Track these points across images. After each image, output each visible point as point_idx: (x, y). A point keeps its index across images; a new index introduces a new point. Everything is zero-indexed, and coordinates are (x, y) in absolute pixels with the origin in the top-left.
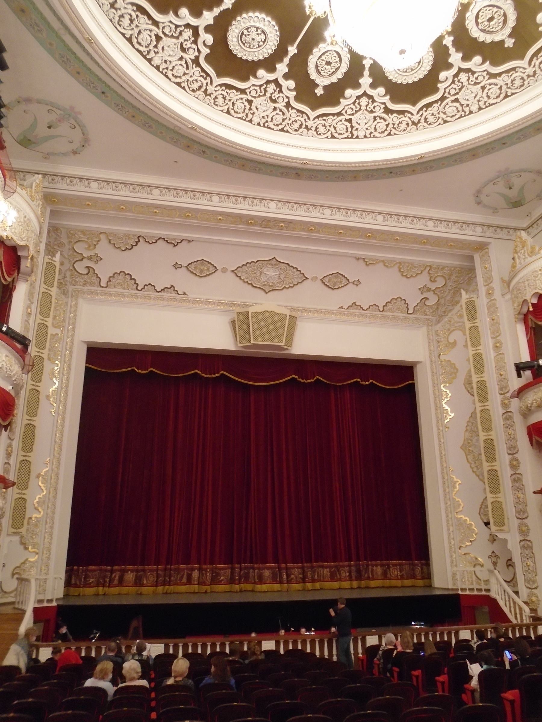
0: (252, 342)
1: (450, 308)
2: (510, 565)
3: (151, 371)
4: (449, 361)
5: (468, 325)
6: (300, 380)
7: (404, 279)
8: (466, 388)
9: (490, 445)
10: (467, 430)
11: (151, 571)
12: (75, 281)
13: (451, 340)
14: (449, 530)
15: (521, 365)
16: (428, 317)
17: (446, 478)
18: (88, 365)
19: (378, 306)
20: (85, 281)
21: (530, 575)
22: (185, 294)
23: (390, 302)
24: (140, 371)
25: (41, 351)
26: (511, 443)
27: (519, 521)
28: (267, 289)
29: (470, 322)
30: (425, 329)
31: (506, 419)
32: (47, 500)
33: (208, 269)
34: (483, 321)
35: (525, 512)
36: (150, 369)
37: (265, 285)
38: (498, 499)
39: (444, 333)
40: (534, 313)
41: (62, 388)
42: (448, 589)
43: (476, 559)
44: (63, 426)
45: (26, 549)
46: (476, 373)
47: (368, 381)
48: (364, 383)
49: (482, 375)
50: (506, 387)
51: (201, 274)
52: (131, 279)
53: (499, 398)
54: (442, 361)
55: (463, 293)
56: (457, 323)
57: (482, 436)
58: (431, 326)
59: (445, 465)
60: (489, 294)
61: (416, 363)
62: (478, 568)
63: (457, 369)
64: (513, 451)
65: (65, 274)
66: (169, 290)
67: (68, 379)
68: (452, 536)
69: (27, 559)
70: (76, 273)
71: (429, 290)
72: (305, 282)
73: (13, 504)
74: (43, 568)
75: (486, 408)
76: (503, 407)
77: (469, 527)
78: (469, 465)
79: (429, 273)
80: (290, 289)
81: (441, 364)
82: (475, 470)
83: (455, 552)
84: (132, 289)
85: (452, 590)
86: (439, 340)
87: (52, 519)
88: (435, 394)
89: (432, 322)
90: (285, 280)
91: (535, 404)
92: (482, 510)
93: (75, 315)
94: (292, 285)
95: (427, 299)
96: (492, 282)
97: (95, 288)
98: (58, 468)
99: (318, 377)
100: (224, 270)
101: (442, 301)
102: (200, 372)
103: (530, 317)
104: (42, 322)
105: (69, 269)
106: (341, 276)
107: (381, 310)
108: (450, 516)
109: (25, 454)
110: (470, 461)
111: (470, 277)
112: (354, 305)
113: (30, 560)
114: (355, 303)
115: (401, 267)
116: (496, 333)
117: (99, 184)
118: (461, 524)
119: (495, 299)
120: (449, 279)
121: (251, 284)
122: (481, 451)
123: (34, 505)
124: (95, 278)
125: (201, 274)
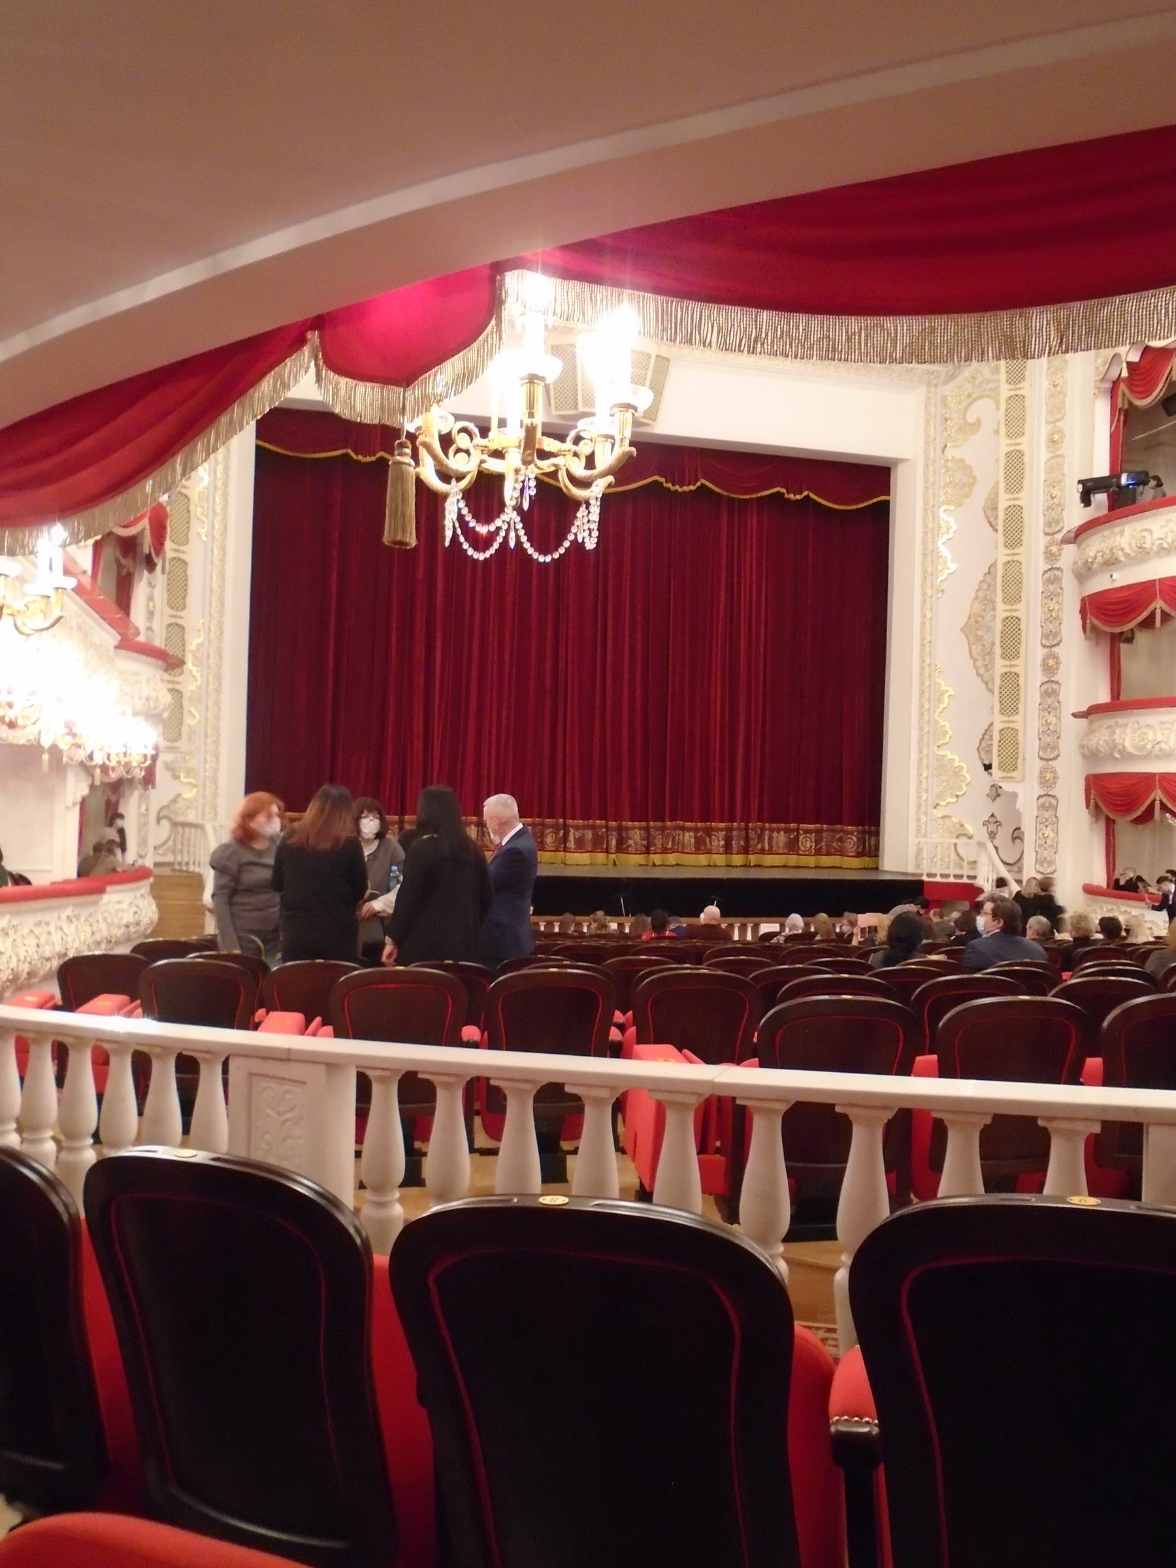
2: (1018, 837)
4: (961, 460)
5: (1005, 391)
6: (669, 485)
8: (987, 517)
9: (1012, 627)
10: (976, 598)
13: (971, 418)
15: (1090, 484)
18: (260, 443)
21: (1046, 853)
24: (360, 458)
26: (1051, 626)
27: (1043, 763)
30: (922, 390)
31: (1049, 582)
35: (1055, 747)
36: (379, 454)
40: (1131, 381)
41: (216, 488)
42: (906, 874)
43: (962, 826)
44: (223, 561)
45: (176, 777)
48: (792, 496)
50: (1058, 522)
53: (1043, 541)
54: (947, 461)
58: (936, 386)
61: (897, 462)
62: (962, 841)
63: (974, 478)
64: (1051, 639)
68: (924, 785)
69: (179, 795)
74: (207, 810)
75: (1015, 558)
76: (1046, 558)
77: (957, 772)
78: (972, 662)
81: (945, 466)
82: (982, 671)
83: (926, 813)
85: (913, 874)
87: (217, 729)
88: (925, 526)
89: (937, 377)
91: (1099, 559)
92: (983, 744)
98: (220, 638)
103: (1123, 387)
108: (925, 752)
109: (173, 612)
110: (976, 656)
116: (1057, 413)
118: (942, 765)
122: (996, 639)
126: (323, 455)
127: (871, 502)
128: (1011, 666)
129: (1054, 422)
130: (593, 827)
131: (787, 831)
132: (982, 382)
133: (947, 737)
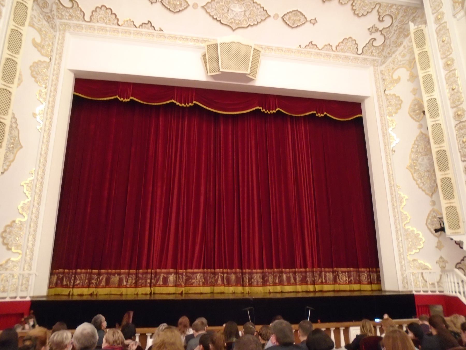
0: (221, 70)
1: (394, 49)
3: (131, 100)
4: (394, 95)
7: (356, 17)
8: (411, 116)
10: (412, 152)
11: (132, 274)
12: (62, 15)
13: (395, 77)
14: (398, 239)
16: (374, 58)
17: (394, 194)
18: (76, 94)
19: (332, 46)
20: (70, 15)
22: (161, 30)
23: (342, 42)
25: (14, 55)
28: (234, 27)
29: (418, 49)
30: (372, 68)
32: (32, 206)
33: (181, 4)
34: (432, 45)
37: (232, 23)
38: (452, 205)
39: (389, 72)
42: (399, 292)
44: (48, 141)
45: (9, 249)
46: (427, 92)
47: (323, 114)
48: (319, 114)
49: (432, 94)
51: (174, 9)
52: (112, 13)
56: (401, 61)
57: (434, 148)
58: (377, 66)
59: (393, 183)
60: (438, 20)
61: (363, 98)
63: (402, 101)
65: (52, 7)
66: (147, 26)
67: (54, 101)
69: (9, 259)
70: (61, 7)
72: (268, 20)
77: (417, 236)
79: (379, 13)
80: (254, 27)
82: (421, 185)
84: (113, 24)
85: (402, 292)
86: (384, 78)
89: (377, 62)
90: (250, 18)
93: (62, 47)
94: (256, 23)
95: (375, 39)
96: (441, 8)
97: (80, 22)
100: (195, 6)
101: (388, 42)
104: (16, 29)
105: (55, 2)
106: (299, 14)
107: (334, 49)
108: (399, 227)
110: (415, 178)
111: (414, 17)
112: (310, 44)
113: (12, 259)
114: (311, 42)
119: (446, 22)
120: (396, 18)
123: (18, 210)
124: (79, 12)
125: (174, 9)
126: (105, 99)
127: (354, 117)
128: (445, 174)
129: (446, 57)
130: (235, 273)
131: (333, 272)
132: (398, 62)
133: (408, 219)
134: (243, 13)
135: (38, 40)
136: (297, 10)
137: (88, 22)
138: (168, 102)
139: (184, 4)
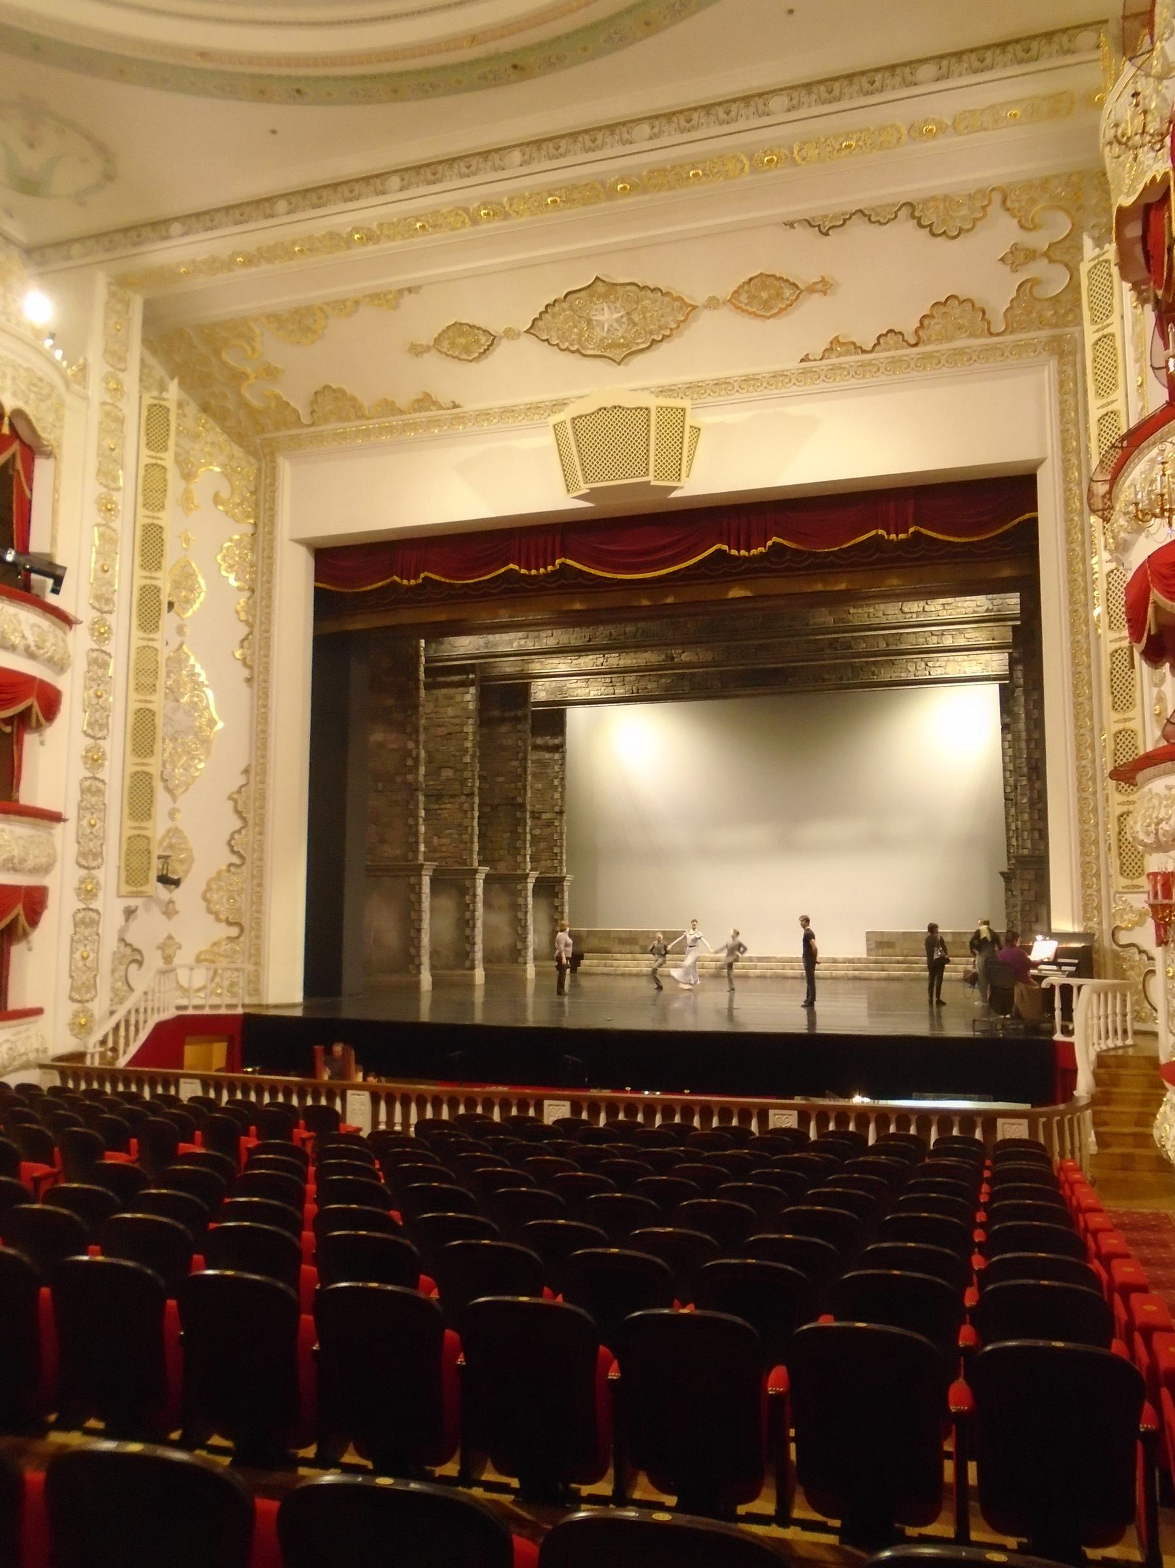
6: (734, 552)
18: (319, 585)
19: (900, 333)
22: (455, 406)
28: (619, 352)
30: (1053, 363)
33: (477, 341)
36: (422, 575)
55: (1088, 242)
71: (1031, 255)
73: (125, 847)
94: (667, 333)
95: (1034, 282)
99: (775, 539)
100: (511, 334)
102: (517, 567)
114: (837, 338)
115: (917, 214)
117: (184, 224)
121: (578, 351)
134: (624, 320)
135: (225, 494)
136: (761, 274)
137: (308, 426)
138: (503, 570)
139: (483, 339)
